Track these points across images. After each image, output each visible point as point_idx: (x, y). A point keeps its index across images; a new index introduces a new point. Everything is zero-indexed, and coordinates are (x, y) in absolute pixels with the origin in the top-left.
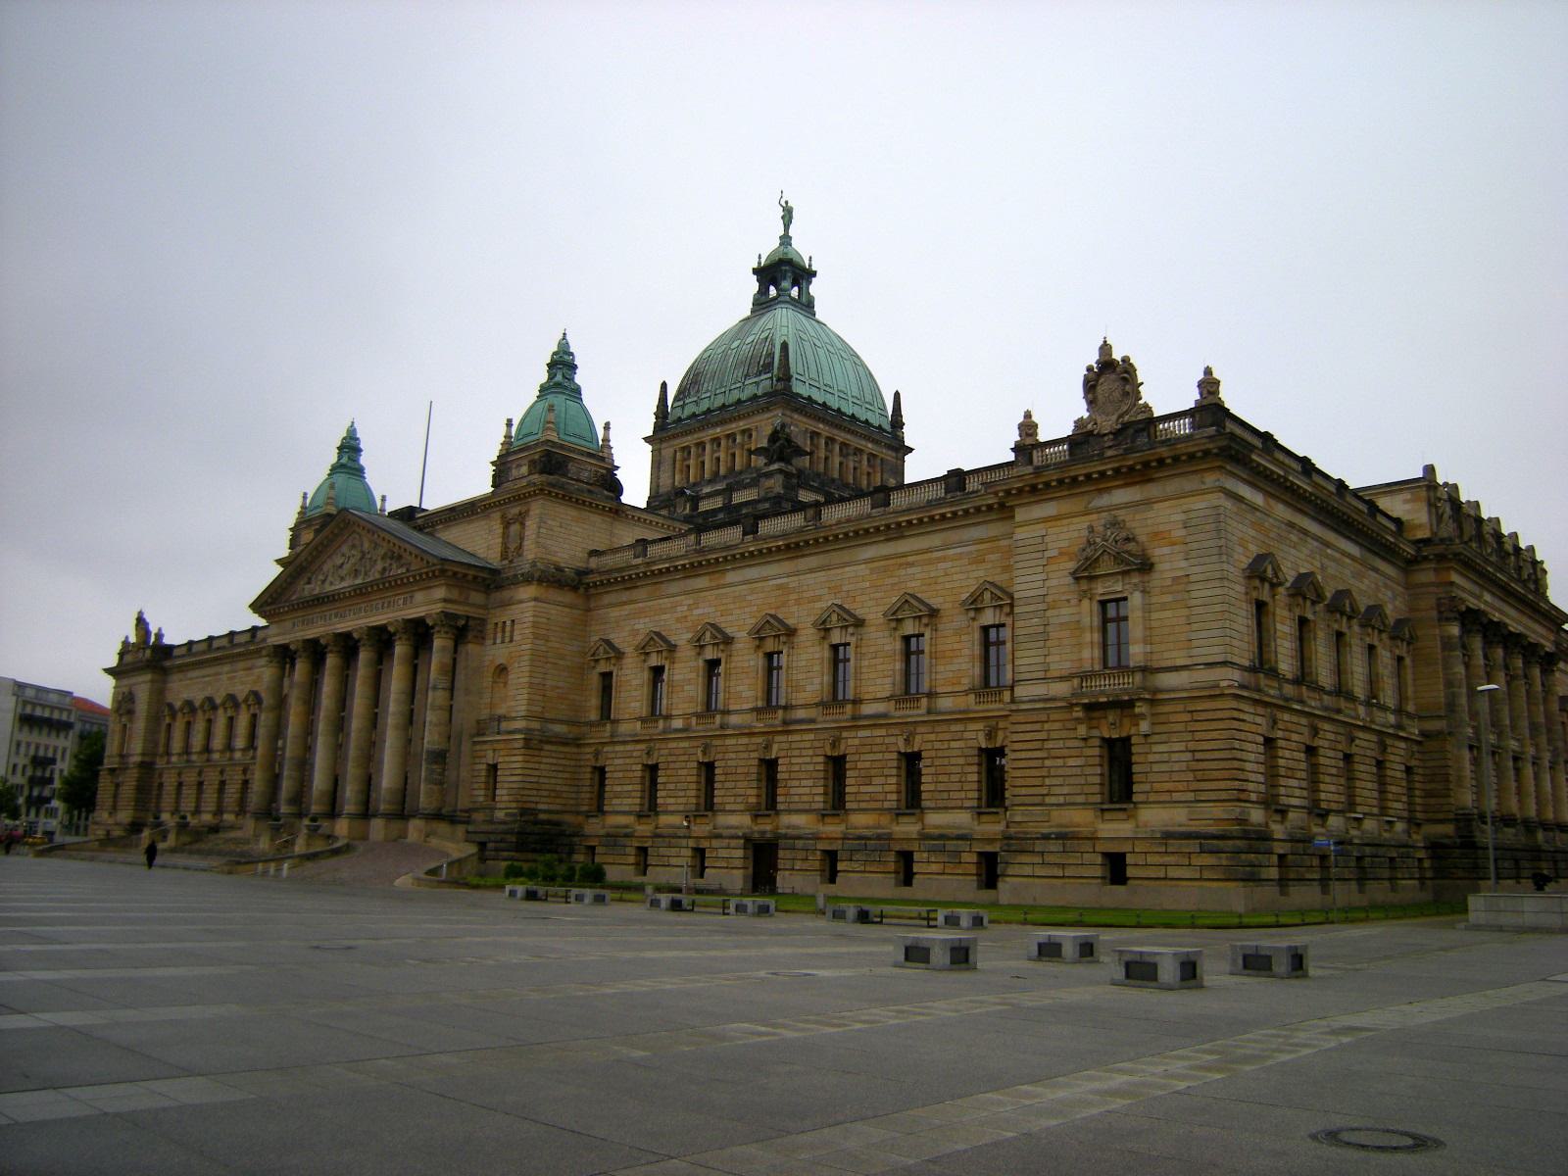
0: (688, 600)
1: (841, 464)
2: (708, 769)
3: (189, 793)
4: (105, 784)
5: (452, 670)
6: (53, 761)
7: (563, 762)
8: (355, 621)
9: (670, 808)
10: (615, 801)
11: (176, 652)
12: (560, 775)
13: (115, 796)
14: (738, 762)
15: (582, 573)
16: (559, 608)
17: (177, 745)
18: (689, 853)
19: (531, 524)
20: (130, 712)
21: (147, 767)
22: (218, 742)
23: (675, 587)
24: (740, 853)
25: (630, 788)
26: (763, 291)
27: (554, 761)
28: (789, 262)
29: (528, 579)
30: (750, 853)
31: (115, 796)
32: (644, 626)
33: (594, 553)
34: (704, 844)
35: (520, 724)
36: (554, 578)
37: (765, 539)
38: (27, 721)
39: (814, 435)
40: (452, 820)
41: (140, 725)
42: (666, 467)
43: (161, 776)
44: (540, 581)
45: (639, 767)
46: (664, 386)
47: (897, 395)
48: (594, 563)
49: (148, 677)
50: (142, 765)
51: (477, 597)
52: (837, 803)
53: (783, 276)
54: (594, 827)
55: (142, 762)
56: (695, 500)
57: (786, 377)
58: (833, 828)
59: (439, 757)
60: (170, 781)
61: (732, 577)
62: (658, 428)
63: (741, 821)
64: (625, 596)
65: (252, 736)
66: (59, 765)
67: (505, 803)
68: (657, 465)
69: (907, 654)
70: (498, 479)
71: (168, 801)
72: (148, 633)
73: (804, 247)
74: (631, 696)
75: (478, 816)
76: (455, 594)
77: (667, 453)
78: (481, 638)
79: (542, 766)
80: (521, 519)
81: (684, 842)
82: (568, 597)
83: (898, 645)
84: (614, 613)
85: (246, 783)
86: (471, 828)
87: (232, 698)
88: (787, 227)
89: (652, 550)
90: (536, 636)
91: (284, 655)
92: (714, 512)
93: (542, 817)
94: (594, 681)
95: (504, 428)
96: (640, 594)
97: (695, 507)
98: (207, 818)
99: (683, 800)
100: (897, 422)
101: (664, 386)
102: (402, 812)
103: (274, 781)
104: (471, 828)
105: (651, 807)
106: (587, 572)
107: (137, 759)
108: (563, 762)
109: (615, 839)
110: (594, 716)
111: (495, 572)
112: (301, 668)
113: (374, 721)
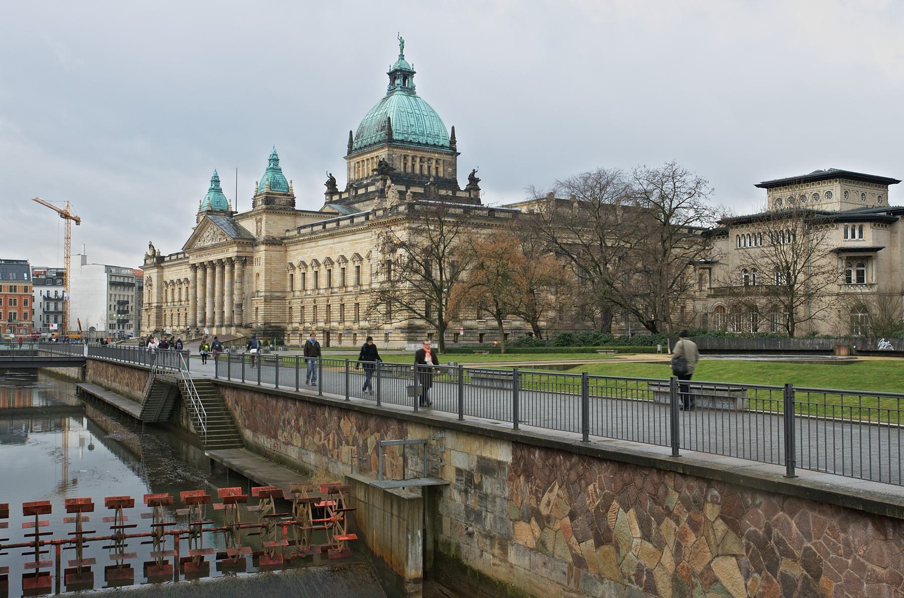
0: (310, 250)
1: (421, 166)
3: (175, 318)
4: (144, 314)
5: (242, 275)
6: (127, 302)
8: (214, 257)
11: (166, 259)
14: (322, 305)
15: (283, 239)
16: (275, 252)
17: (170, 299)
19: (263, 222)
20: (151, 285)
22: (183, 298)
23: (307, 245)
26: (393, 82)
28: (401, 70)
29: (263, 243)
32: (301, 258)
33: (288, 231)
35: (263, 294)
36: (271, 242)
37: (329, 231)
38: (112, 284)
39: (405, 157)
40: (247, 327)
41: (155, 290)
42: (352, 170)
44: (266, 244)
46: (351, 132)
47: (453, 128)
48: (287, 234)
49: (156, 270)
50: (157, 307)
51: (249, 249)
52: (342, 320)
53: (401, 77)
54: (289, 327)
56: (356, 189)
57: (390, 133)
58: (341, 327)
59: (240, 306)
60: (168, 313)
61: (321, 243)
62: (350, 152)
63: (321, 325)
64: (295, 247)
65: (187, 295)
66: (130, 305)
67: (260, 322)
68: (349, 169)
69: (344, 274)
70: (254, 205)
71: (168, 322)
72: (154, 251)
73: (410, 61)
74: (298, 285)
75: (254, 325)
76: (241, 249)
77: (352, 164)
78: (252, 263)
80: (261, 219)
82: (278, 248)
83: (355, 269)
84: (293, 253)
87: (186, 279)
88: (402, 51)
89: (302, 231)
90: (266, 263)
91: (194, 267)
92: (362, 194)
94: (289, 277)
95: (255, 186)
96: (299, 247)
97: (356, 192)
98: (182, 328)
100: (453, 141)
101: (351, 132)
102: (230, 326)
105: (302, 322)
106: (285, 238)
109: (295, 330)
110: (289, 289)
111: (254, 239)
112: (200, 273)
113: (223, 294)
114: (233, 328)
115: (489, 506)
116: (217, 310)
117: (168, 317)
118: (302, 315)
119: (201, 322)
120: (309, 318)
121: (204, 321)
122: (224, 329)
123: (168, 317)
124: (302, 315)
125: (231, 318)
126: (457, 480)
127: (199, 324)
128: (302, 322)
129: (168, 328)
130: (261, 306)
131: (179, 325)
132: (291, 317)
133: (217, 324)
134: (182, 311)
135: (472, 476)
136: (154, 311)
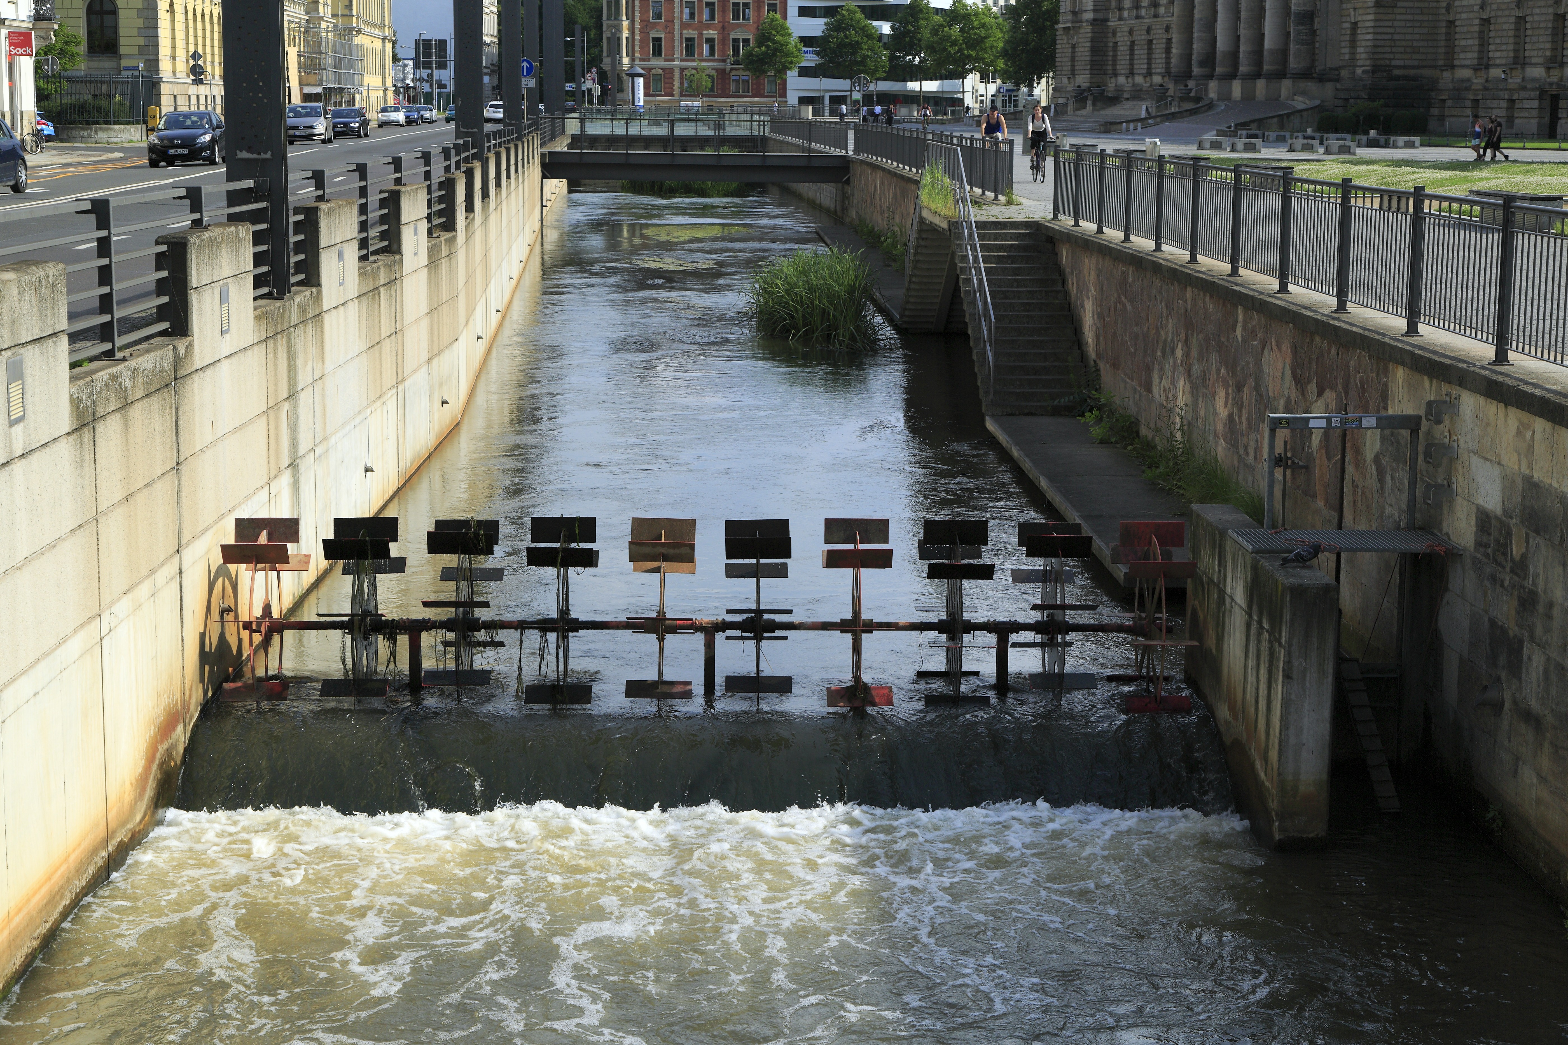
2: (1521, 20)
3: (1141, 52)
7: (1420, 18)
9: (1498, 62)
10: (1462, 56)
12: (1416, 30)
13: (1073, 59)
18: (1504, 104)
21: (1099, 23)
24: (1535, 104)
25: (1470, 42)
27: (1410, 17)
30: (1547, 103)
31: (1073, 59)
34: (1515, 97)
40: (1322, 79)
43: (1114, 33)
45: (1477, 22)
50: (1094, 22)
55: (1095, 20)
60: (1123, 39)
63: (1536, 72)
75: (1344, 73)
79: (1396, 24)
81: (1501, 93)
85: (1169, 41)
86: (1339, 86)
93: (1397, 72)
99: (1505, 54)
102: (1280, 74)
103: (1188, 43)
104: (1339, 86)
105: (1483, 64)
107: (1089, 16)
108: (1420, 18)
109: (1460, 90)
114: (1286, 85)
115: (1539, 631)
116: (1243, 32)
117: (1123, 48)
118: (1484, 43)
119: (1202, 64)
120: (1501, 53)
121: (1209, 60)
122: (1261, 84)
123: (1123, 48)
124: (1484, 43)
125: (1283, 53)
126: (1479, 544)
127: (1196, 70)
128: (1483, 64)
129: (1122, 80)
130: (1367, 20)
131: (1149, 73)
132: (1451, 51)
133: (1243, 69)
134: (1159, 34)
135: (1509, 534)
136: (1087, 29)
